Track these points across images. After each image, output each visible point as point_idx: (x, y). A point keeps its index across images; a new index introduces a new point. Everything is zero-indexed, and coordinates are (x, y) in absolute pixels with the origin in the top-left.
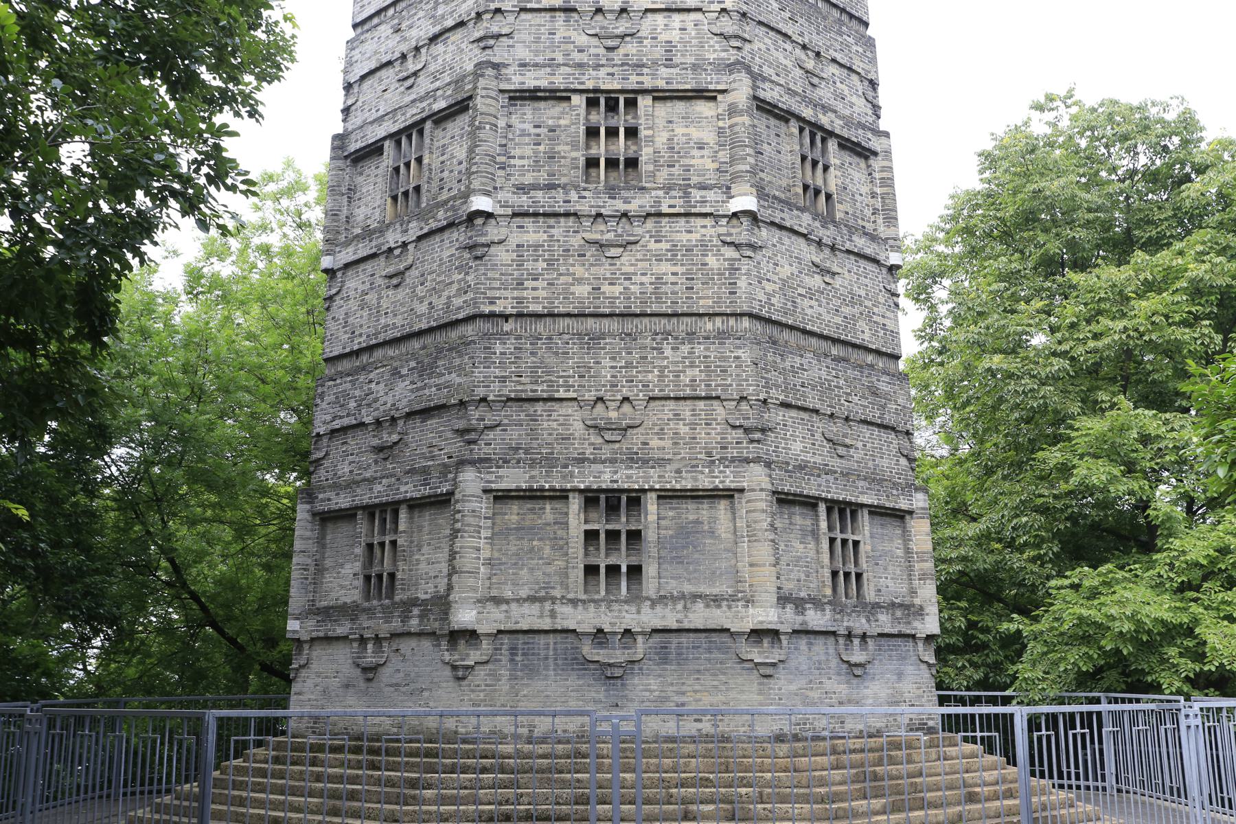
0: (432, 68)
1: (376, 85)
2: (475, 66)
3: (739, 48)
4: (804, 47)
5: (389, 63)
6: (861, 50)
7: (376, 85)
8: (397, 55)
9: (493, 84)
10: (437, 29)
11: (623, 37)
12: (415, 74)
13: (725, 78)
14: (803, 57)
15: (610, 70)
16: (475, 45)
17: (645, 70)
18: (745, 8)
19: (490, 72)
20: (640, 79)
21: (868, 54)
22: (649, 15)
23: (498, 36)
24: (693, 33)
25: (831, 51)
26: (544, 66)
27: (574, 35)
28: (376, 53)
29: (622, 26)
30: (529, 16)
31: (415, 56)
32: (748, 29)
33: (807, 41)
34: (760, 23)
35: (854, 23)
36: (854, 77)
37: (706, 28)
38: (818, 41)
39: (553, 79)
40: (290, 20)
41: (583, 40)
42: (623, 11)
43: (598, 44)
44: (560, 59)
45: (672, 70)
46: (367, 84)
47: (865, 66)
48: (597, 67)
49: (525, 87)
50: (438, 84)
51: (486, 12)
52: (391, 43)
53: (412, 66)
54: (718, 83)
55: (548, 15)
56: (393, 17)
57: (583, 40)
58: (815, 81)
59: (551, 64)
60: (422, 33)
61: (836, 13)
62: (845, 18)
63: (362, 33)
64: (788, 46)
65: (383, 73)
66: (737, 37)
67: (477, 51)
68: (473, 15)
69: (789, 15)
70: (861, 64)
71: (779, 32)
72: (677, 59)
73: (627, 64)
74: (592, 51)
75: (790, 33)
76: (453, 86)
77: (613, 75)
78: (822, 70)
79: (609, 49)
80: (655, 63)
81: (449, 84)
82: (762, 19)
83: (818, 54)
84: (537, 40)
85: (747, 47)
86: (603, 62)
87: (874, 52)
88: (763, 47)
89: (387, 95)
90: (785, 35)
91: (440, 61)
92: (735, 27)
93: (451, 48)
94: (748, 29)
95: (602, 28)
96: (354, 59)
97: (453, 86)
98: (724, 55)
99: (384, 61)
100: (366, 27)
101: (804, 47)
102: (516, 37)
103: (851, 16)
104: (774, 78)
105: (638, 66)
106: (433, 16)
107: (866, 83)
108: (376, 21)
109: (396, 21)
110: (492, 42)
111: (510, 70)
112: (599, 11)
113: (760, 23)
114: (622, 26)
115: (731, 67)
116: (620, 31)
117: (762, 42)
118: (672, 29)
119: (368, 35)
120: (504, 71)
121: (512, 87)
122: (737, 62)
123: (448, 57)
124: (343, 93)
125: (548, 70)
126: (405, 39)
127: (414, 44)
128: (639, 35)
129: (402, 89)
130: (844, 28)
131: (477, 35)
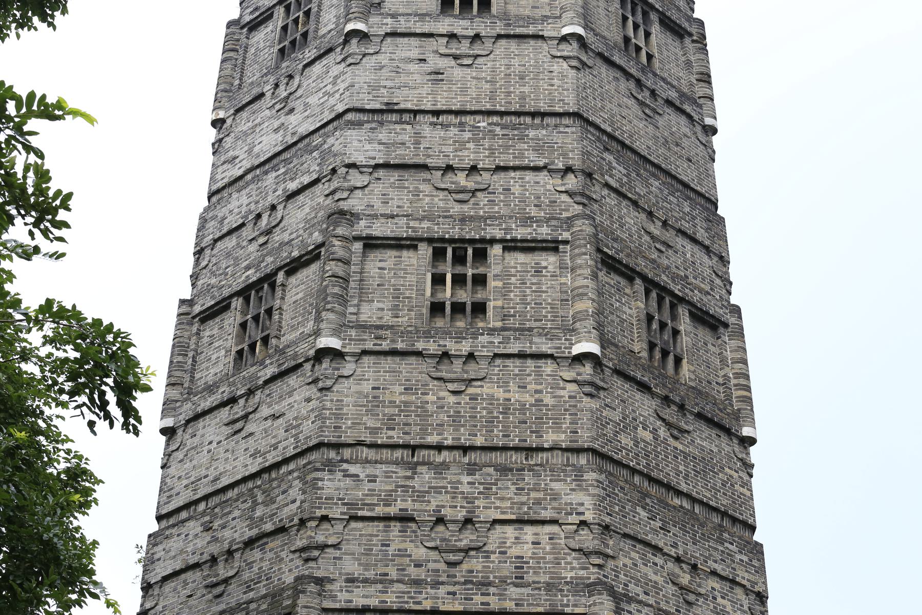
0: (246, 576)
1: (179, 588)
2: (297, 579)
3: (600, 566)
4: (678, 560)
5: (196, 566)
6: (745, 559)
7: (179, 588)
8: (206, 557)
9: (315, 602)
10: (254, 532)
11: (466, 551)
12: (226, 581)
13: (583, 600)
14: (677, 570)
15: (451, 588)
16: (297, 555)
17: (492, 590)
18: (607, 519)
19: (312, 588)
20: (486, 599)
21: (755, 563)
22: (497, 527)
23: (323, 547)
24: (548, 548)
25: (710, 563)
26: (375, 582)
27: (410, 547)
28: (182, 552)
29: (467, 538)
30: (360, 525)
31: (226, 560)
32: (611, 543)
33: (681, 552)
34: (626, 536)
35: (737, 529)
36: (739, 591)
37: (562, 542)
38: (694, 552)
39: (384, 597)
40: (113, 605)
41: (421, 553)
42: (468, 521)
43: (438, 557)
44: (393, 574)
45: (523, 590)
46: (169, 586)
47: (752, 578)
48: (436, 584)
49: (352, 606)
50: (251, 595)
51: (311, 519)
52: (200, 543)
53: (223, 571)
54: (575, 606)
55: (381, 525)
56: (204, 513)
57: (421, 553)
58: (691, 598)
59: (384, 580)
60: (236, 535)
61: (716, 519)
62: (726, 523)
63: (168, 528)
64: (659, 560)
65: (189, 576)
66: (598, 553)
67: (299, 562)
68: (296, 521)
69: (659, 524)
70: (746, 575)
71: (647, 544)
72: (530, 577)
73: (471, 582)
74: (431, 566)
75: (661, 544)
76: (269, 600)
77: (454, 594)
78: (699, 586)
79: (451, 564)
80: (503, 581)
81: (264, 597)
82: (627, 531)
83: (694, 567)
84: (368, 552)
85: (611, 563)
86: (443, 578)
87: (761, 560)
88: (629, 562)
89: (192, 602)
90: (657, 549)
91: (255, 569)
92: (596, 542)
93: (270, 555)
94: (611, 543)
95: (443, 540)
96: (156, 557)
97: (269, 600)
98: (582, 573)
99: (191, 562)
100: (172, 521)
101: (678, 560)
102: (344, 547)
103: (734, 520)
104: (642, 597)
105: (483, 584)
106: (251, 518)
107: (753, 597)
108: (184, 515)
109: (207, 518)
110: (316, 553)
111: (336, 586)
112: (440, 521)
113: (626, 536)
114: (467, 538)
115: (590, 588)
116: (463, 544)
117: (628, 557)
118: (523, 543)
119: (174, 531)
120: (328, 587)
121: (337, 606)
122: (599, 582)
123: (265, 565)
124: (141, 593)
125: (380, 587)
126: (215, 540)
127: (226, 546)
128: (485, 548)
129: (210, 596)
130: (726, 535)
131: (299, 544)
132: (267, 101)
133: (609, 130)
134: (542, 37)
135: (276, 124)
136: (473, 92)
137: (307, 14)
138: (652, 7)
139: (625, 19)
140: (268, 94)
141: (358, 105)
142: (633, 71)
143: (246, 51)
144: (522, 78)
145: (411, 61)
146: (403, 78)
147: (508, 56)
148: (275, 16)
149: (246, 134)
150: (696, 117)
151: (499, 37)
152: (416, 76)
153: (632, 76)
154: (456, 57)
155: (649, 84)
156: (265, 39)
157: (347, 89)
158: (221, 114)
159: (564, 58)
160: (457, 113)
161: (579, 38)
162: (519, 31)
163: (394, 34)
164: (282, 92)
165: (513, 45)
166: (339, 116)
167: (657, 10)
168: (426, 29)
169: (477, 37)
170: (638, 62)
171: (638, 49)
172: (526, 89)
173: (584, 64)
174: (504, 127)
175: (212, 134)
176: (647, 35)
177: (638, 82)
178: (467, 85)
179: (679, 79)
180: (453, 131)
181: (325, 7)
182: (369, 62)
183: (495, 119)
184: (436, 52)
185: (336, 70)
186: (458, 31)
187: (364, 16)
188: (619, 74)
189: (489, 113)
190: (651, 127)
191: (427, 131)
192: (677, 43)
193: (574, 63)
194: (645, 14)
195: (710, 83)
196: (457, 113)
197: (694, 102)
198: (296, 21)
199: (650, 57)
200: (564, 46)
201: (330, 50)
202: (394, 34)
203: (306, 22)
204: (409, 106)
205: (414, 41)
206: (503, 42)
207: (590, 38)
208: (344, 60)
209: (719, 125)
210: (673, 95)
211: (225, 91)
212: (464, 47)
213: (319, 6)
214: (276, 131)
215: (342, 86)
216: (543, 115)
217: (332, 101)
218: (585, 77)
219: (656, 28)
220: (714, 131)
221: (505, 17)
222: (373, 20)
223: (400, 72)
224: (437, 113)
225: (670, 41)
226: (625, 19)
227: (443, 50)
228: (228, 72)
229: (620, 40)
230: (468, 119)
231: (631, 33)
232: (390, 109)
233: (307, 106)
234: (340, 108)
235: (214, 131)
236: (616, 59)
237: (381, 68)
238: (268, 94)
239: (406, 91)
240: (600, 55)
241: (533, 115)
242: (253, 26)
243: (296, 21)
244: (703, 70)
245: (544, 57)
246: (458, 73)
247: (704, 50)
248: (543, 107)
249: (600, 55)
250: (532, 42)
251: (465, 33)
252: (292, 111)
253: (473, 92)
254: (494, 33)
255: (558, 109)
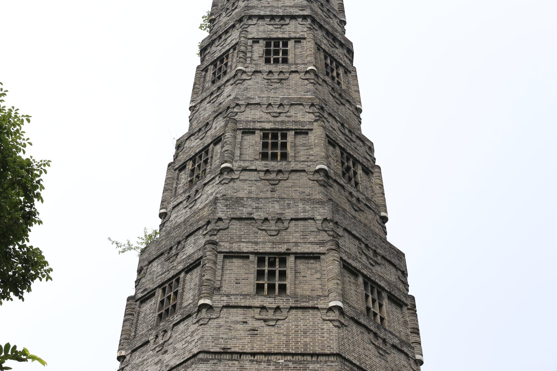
132: (151, 346)
133: (358, 363)
134: (317, 308)
135: (156, 360)
136: (275, 342)
137: (176, 293)
138: (383, 289)
139: (367, 296)
140: (152, 342)
141: (206, 349)
142: (372, 328)
143: (138, 315)
144: (305, 333)
145: (237, 322)
146: (233, 333)
147: (296, 320)
148: (156, 294)
149: (138, 365)
150: (410, 355)
151: (291, 308)
152: (241, 332)
153: (371, 331)
154: (265, 321)
155: (382, 335)
156: (150, 308)
157: (199, 339)
158: (123, 353)
159: (331, 321)
160: (266, 354)
161: (339, 308)
162: (303, 304)
163: (228, 307)
164: (160, 341)
165: (300, 313)
166: (194, 356)
167: (386, 291)
168: (247, 303)
169: (278, 308)
170: (375, 322)
171: (375, 314)
172: (308, 340)
173: (342, 324)
174: (294, 362)
175: (118, 365)
176: (381, 306)
177: (375, 334)
178: (272, 338)
179: (400, 332)
180: (264, 365)
181: (186, 290)
182: (213, 323)
183: (289, 358)
184: (253, 317)
185: (193, 328)
186: (266, 305)
187: (210, 296)
188: (363, 330)
189: (285, 354)
190: (383, 362)
191: (247, 365)
192: (399, 310)
193: (337, 324)
194: (379, 293)
195: (418, 334)
196: (266, 354)
197: (409, 345)
198: (169, 298)
199: (382, 319)
200: (330, 313)
201: (189, 316)
202: (228, 307)
203: (175, 299)
204: (237, 350)
205: (240, 311)
206: (294, 311)
207: (346, 308)
208: (197, 322)
209: (425, 359)
210: (396, 342)
211: (126, 339)
212: (270, 315)
213: (183, 289)
214: (156, 364)
215: (196, 338)
216: (318, 355)
217: (190, 346)
218: (343, 332)
219: (385, 302)
220: (421, 363)
221: (295, 296)
222: (215, 298)
223: (232, 330)
224: (254, 354)
225: (394, 309)
226: (367, 296)
227: (257, 316)
228: (127, 328)
229: (364, 309)
230: (273, 358)
231: (371, 305)
232: (225, 352)
233: (175, 349)
234: (195, 351)
235: (119, 363)
236: (362, 321)
237: (220, 327)
238: (152, 342)
239: (235, 341)
240: (352, 319)
241: (312, 355)
242: (143, 300)
243: (169, 298)
244: (415, 326)
245: (318, 320)
246: (266, 330)
247: (415, 314)
248: (318, 350)
249: (352, 319)
250: (311, 311)
251: (271, 306)
252: (166, 352)
253: (275, 342)
254: (288, 306)
255: (327, 351)
